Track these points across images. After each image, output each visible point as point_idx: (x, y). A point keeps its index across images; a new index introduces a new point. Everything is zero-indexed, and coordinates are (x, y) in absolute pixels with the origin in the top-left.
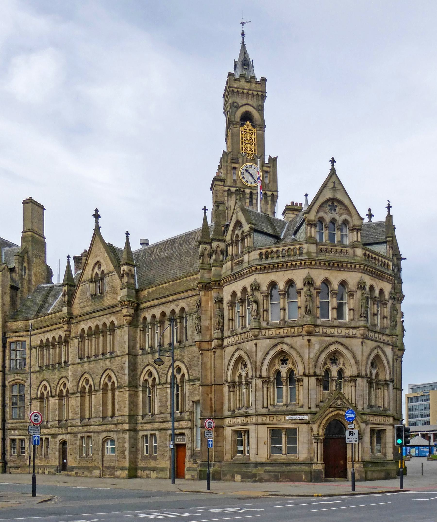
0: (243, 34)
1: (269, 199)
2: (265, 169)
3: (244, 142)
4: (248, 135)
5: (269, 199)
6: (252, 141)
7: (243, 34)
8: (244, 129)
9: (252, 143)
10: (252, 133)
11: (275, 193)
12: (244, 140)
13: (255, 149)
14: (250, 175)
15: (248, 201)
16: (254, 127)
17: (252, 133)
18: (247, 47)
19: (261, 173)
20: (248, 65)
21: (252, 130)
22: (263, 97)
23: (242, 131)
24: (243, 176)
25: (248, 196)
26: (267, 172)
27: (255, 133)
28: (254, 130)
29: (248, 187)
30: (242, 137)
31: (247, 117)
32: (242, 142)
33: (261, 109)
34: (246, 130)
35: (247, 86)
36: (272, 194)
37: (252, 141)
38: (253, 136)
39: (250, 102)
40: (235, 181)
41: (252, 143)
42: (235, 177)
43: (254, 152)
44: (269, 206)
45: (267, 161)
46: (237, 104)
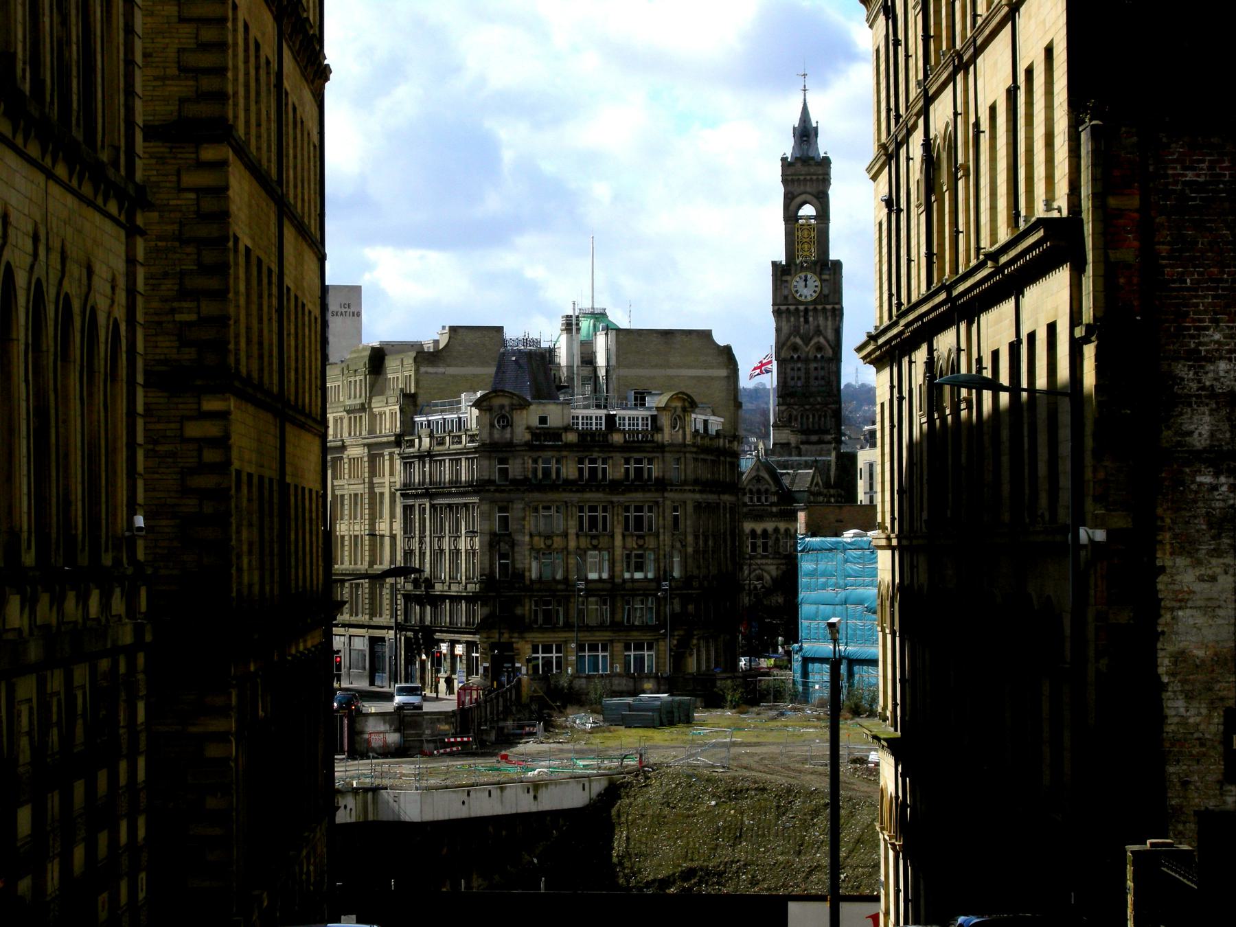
1: (829, 314)
2: (825, 277)
4: (806, 232)
5: (829, 314)
15: (802, 319)
18: (809, 105)
19: (818, 283)
26: (825, 280)
29: (801, 303)
35: (804, 170)
36: (834, 309)
39: (808, 190)
40: (786, 297)
42: (785, 292)
44: (829, 323)
46: (792, 193)
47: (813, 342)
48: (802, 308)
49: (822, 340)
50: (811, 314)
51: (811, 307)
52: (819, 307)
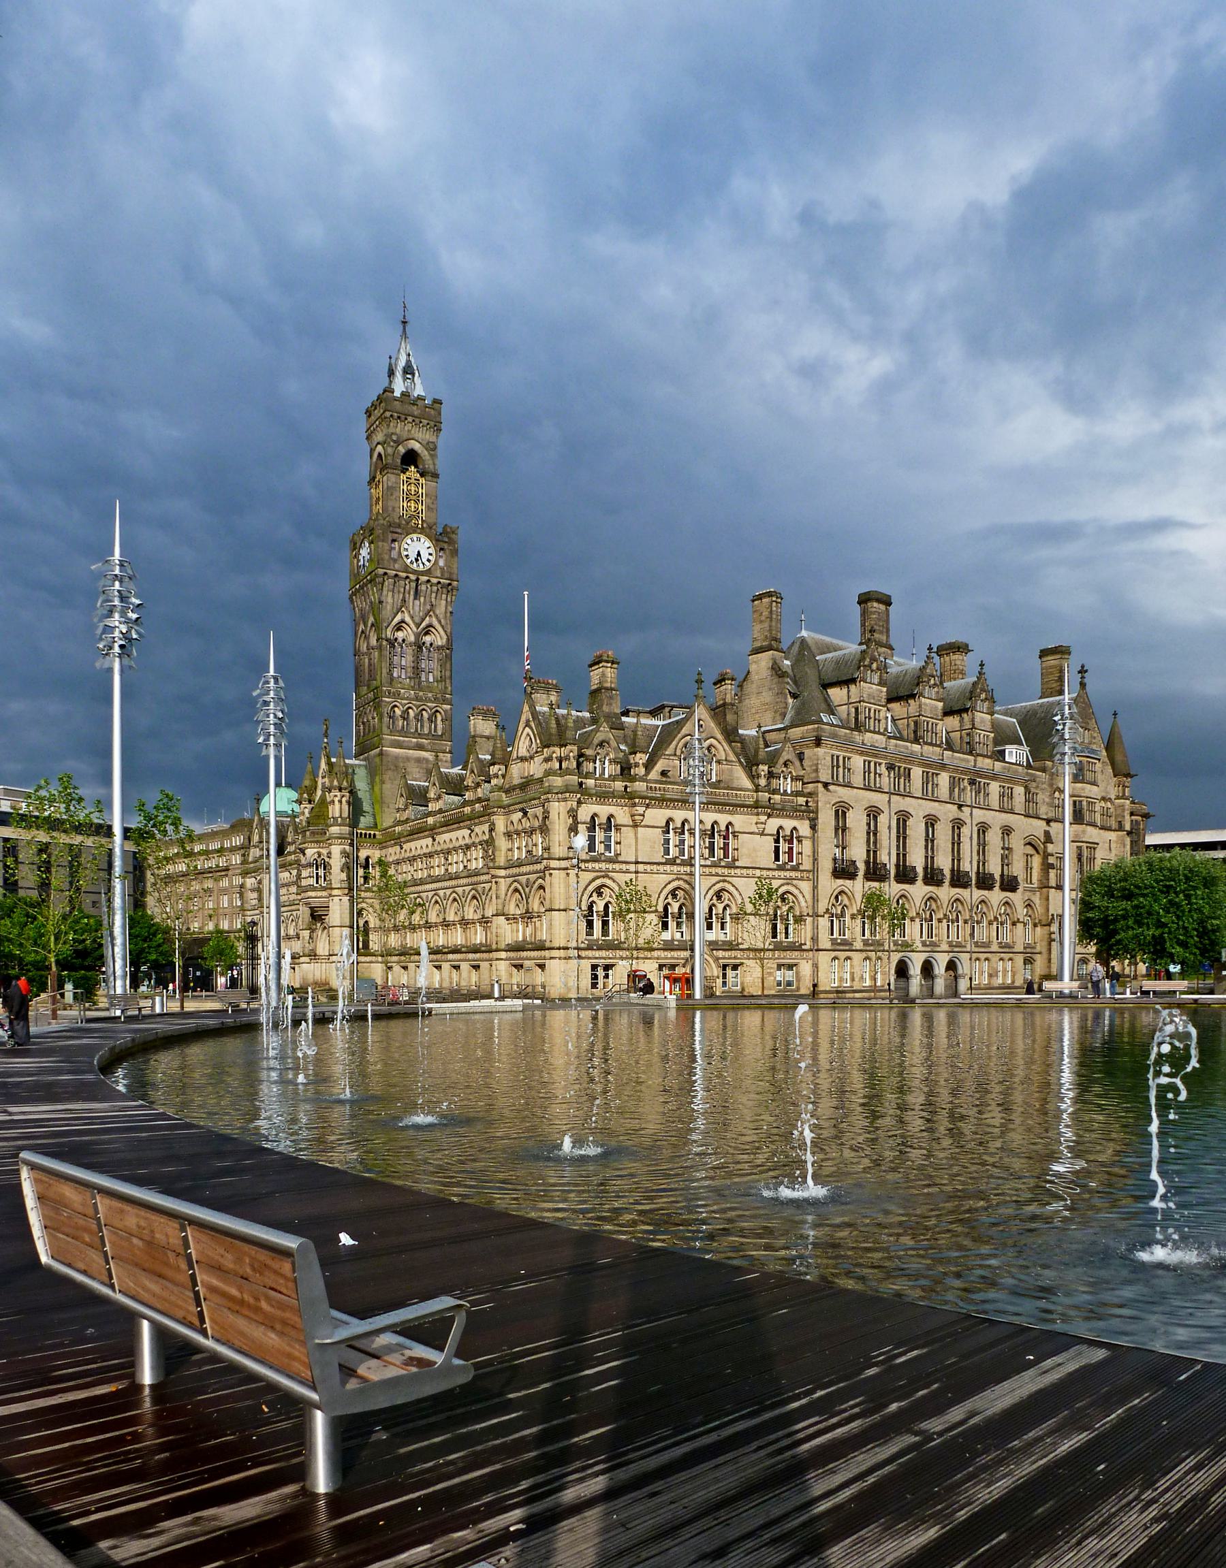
0: (404, 323)
7: (404, 323)
16: (422, 475)
20: (413, 375)
25: (413, 585)
28: (422, 481)
31: (411, 458)
33: (432, 448)
45: (440, 530)
47: (424, 625)
48: (413, 577)
49: (435, 623)
50: (423, 587)
52: (434, 581)
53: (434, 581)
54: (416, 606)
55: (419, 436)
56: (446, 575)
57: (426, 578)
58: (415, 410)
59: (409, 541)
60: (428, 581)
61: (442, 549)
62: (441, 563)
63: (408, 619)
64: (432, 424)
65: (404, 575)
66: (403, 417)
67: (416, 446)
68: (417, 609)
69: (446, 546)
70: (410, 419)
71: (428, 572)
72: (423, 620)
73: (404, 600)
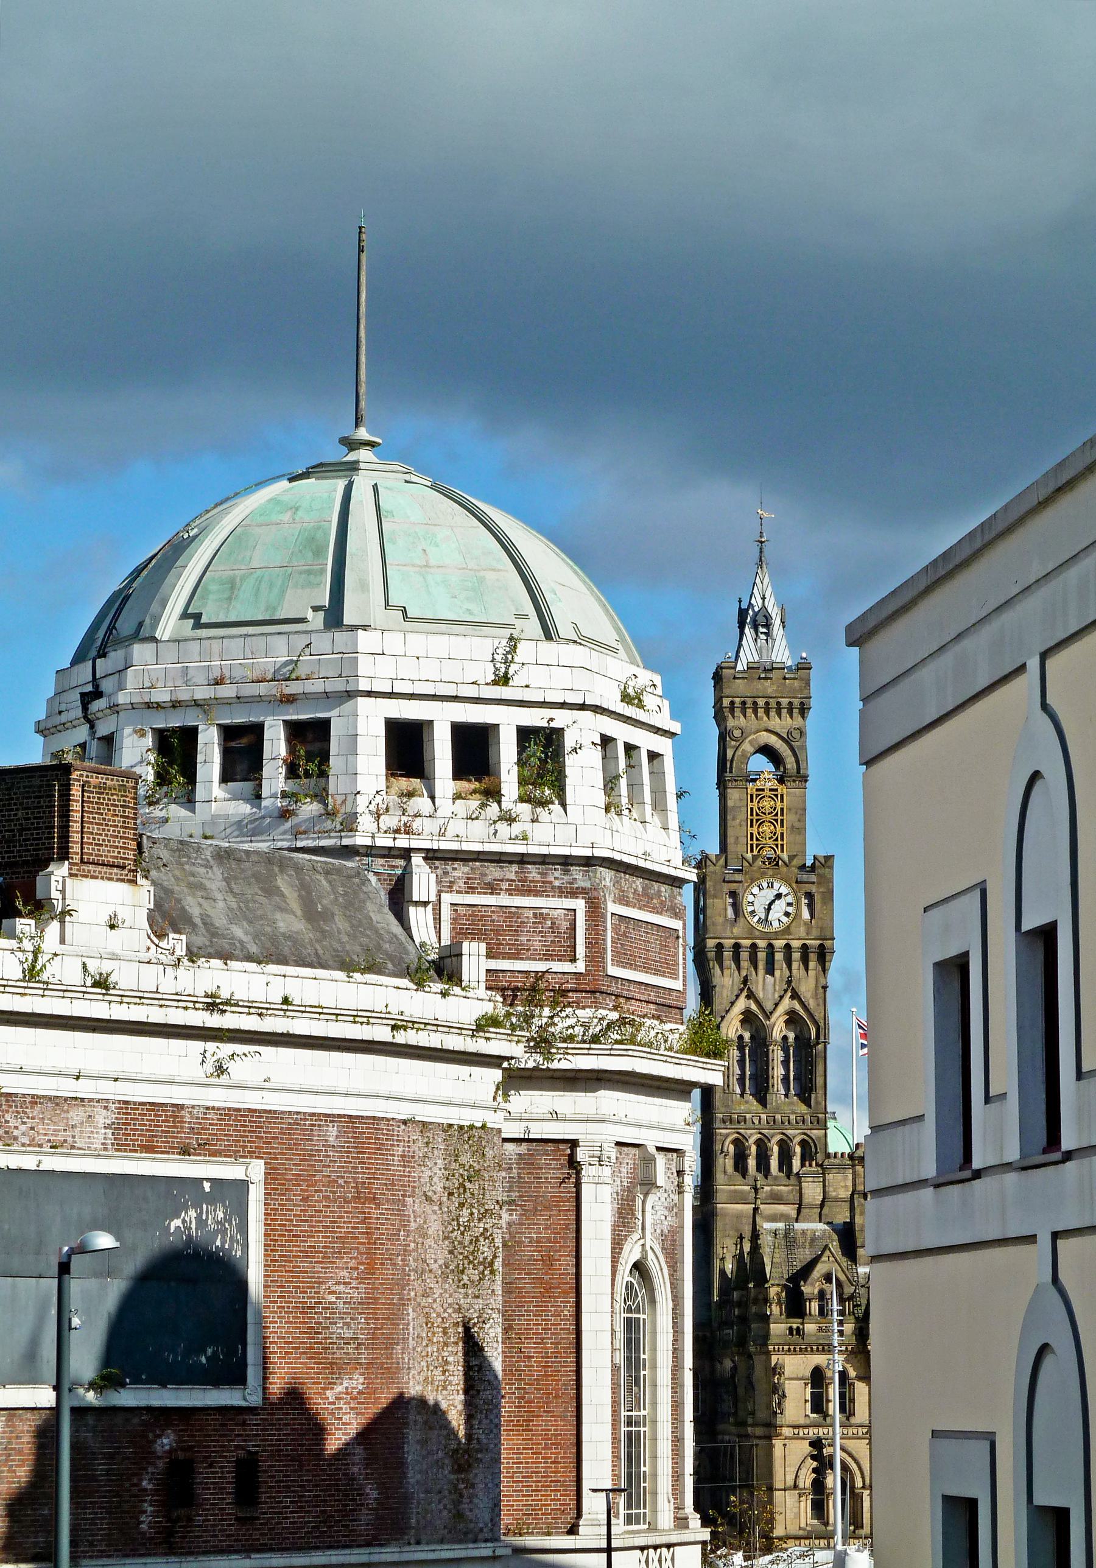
3: (757, 820)
4: (767, 804)
6: (776, 815)
8: (757, 790)
9: (776, 821)
10: (776, 796)
11: (827, 943)
12: (757, 815)
13: (782, 834)
14: (769, 903)
16: (781, 781)
17: (776, 796)
21: (776, 790)
22: (804, 710)
23: (752, 796)
24: (750, 909)
25: (762, 956)
27: (782, 796)
28: (782, 789)
29: (764, 936)
30: (752, 809)
32: (752, 820)
34: (763, 790)
36: (821, 946)
37: (776, 815)
38: (779, 803)
41: (776, 821)
43: (780, 842)
50: (779, 957)
51: (779, 944)
52: (796, 944)
53: (796, 944)
54: (767, 986)
55: (775, 722)
56: (815, 933)
57: (783, 942)
58: (769, 688)
59: (755, 890)
60: (788, 947)
61: (809, 896)
62: (806, 914)
63: (754, 1007)
64: (796, 702)
65: (746, 943)
66: (749, 701)
67: (773, 740)
68: (770, 988)
69: (813, 889)
70: (761, 702)
71: (787, 930)
72: (777, 1005)
73: (745, 981)
